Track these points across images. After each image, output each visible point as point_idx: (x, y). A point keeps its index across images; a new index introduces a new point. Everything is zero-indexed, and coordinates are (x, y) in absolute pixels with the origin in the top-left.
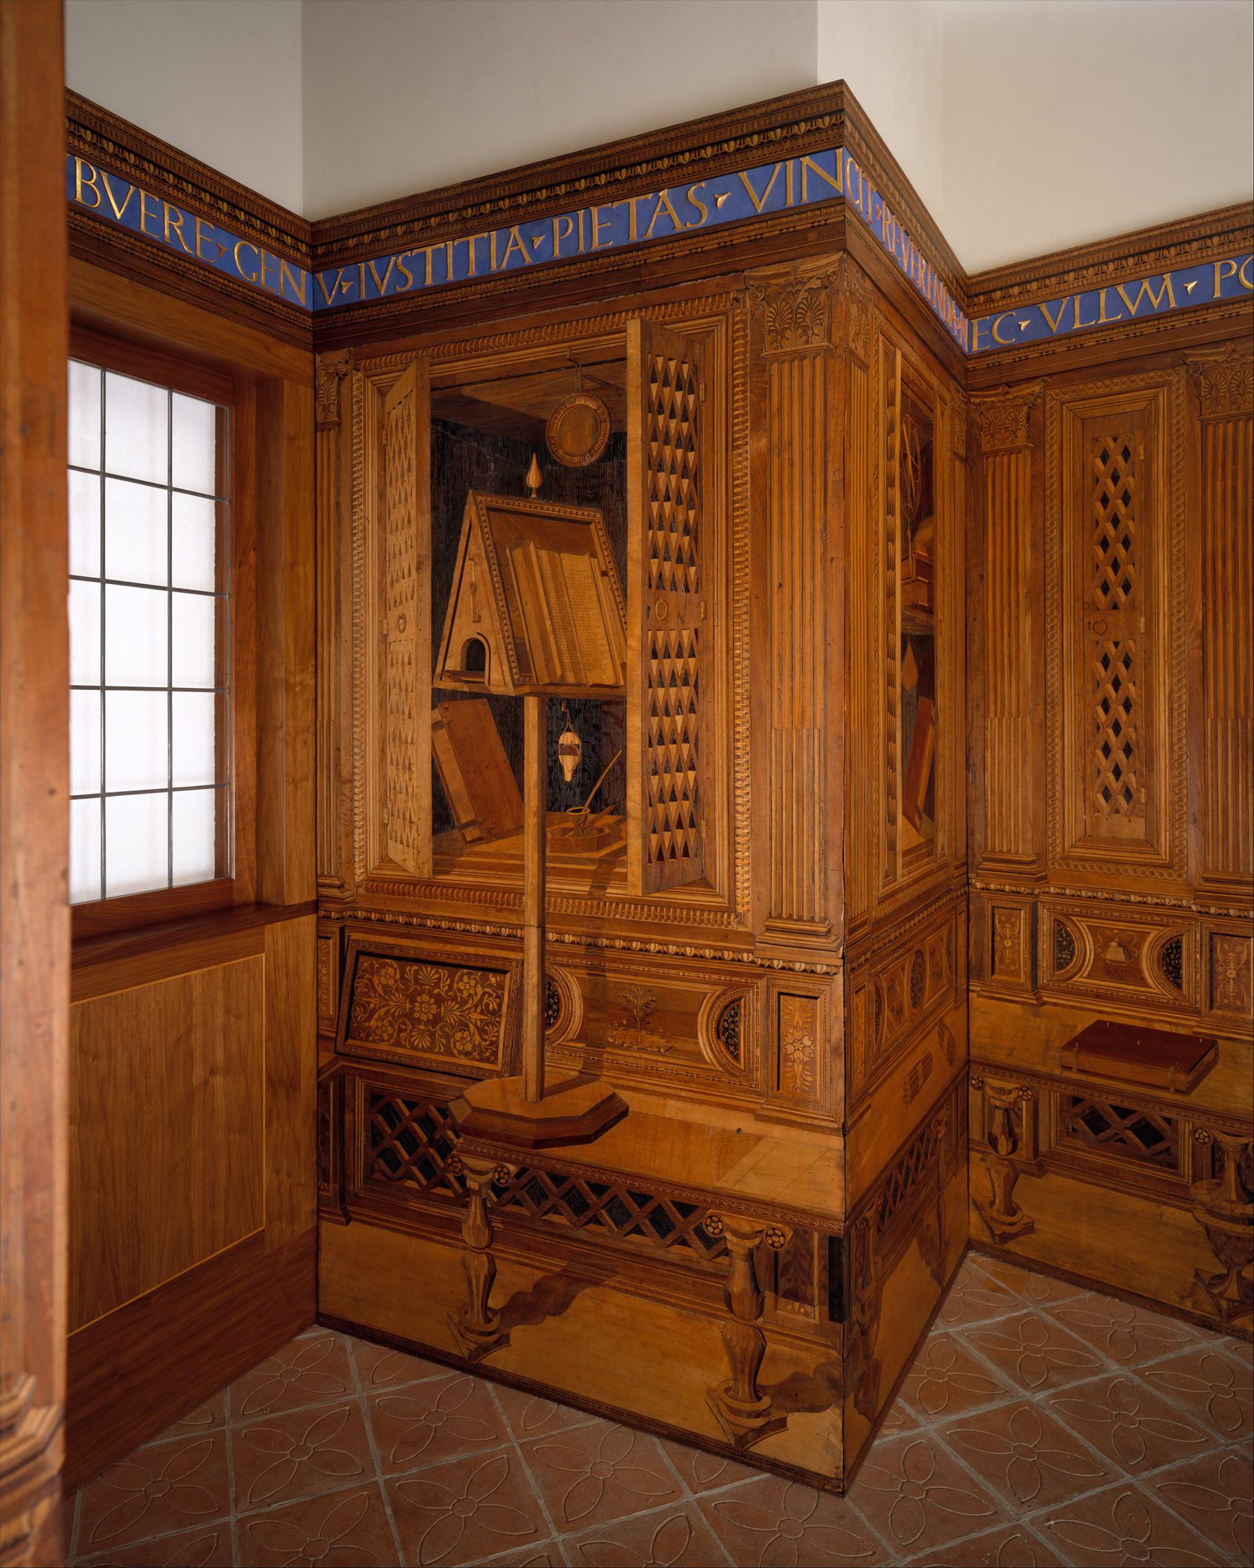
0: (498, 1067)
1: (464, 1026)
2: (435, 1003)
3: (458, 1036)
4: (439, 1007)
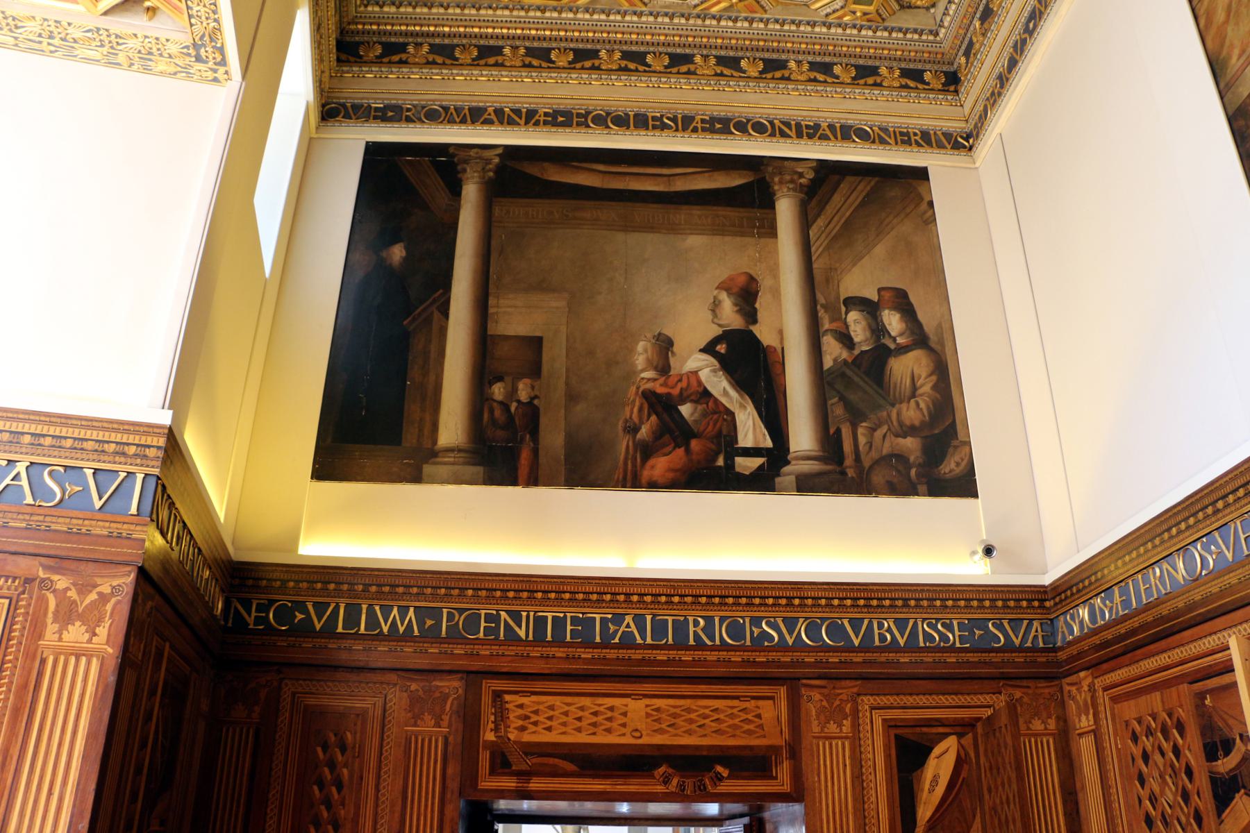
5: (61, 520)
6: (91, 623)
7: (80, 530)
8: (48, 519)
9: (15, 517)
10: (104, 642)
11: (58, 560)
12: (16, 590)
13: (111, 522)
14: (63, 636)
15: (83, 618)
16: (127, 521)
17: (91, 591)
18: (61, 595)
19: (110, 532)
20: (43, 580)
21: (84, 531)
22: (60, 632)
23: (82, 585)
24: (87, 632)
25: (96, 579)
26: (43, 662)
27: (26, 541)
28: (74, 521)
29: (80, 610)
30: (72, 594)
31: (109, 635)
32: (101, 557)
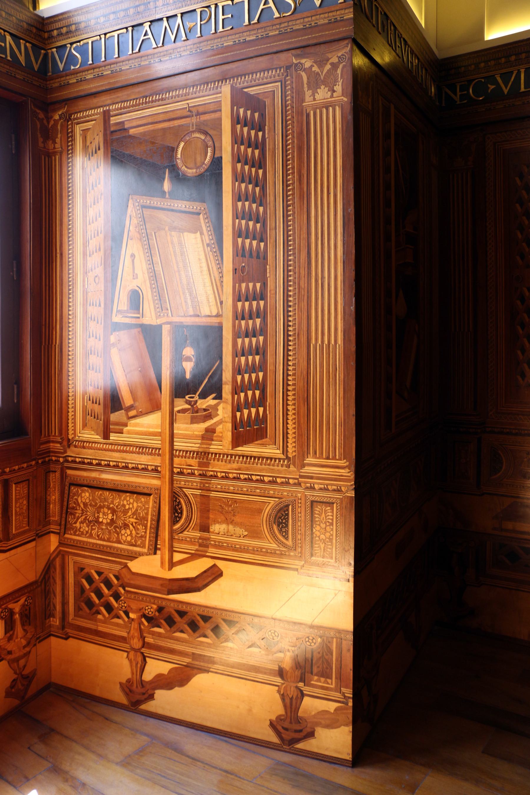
0: (145, 550)
1: (126, 526)
2: (111, 513)
3: (123, 532)
4: (113, 515)
5: (298, 22)
6: (330, 85)
7: (311, 24)
8: (290, 23)
9: (271, 29)
10: (341, 94)
11: (302, 49)
12: (283, 75)
13: (328, 13)
14: (316, 97)
15: (325, 83)
16: (338, 8)
17: (326, 64)
18: (308, 71)
19: (329, 20)
20: (296, 65)
21: (313, 24)
22: (313, 95)
23: (320, 61)
24: (329, 91)
25: (327, 55)
26: (308, 115)
27: (281, 42)
28: (306, 20)
29: (322, 77)
30: (315, 69)
31: (343, 90)
32: (328, 39)
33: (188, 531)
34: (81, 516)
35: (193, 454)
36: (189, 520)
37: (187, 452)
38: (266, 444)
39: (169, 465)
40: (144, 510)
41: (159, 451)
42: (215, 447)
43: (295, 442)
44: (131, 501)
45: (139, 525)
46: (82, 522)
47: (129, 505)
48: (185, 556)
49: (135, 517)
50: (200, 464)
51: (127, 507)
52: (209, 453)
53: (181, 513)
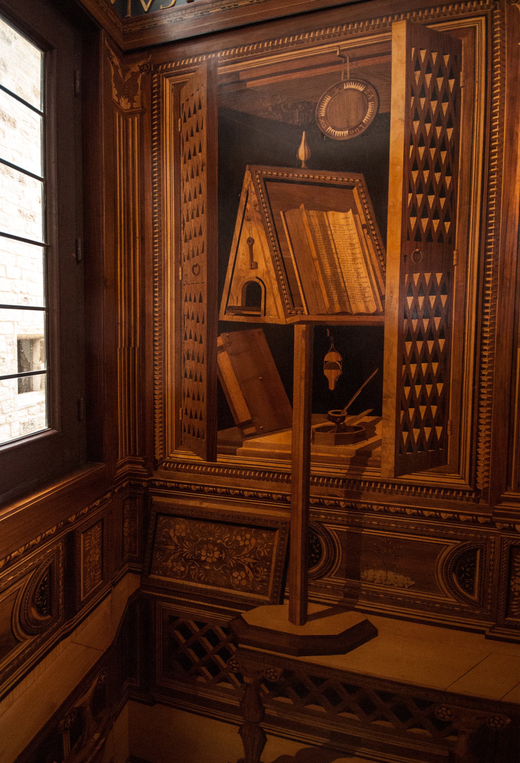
1: (240, 567)
4: (221, 553)
33: (328, 577)
34: (174, 553)
35: (338, 482)
36: (331, 562)
37: (329, 479)
38: (446, 472)
39: (303, 495)
40: (266, 548)
41: (288, 477)
42: (369, 474)
43: (487, 471)
44: (248, 536)
45: (259, 566)
46: (175, 560)
47: (245, 541)
48: (326, 608)
49: (253, 557)
50: (348, 494)
51: (242, 544)
52: (361, 481)
53: (320, 554)
